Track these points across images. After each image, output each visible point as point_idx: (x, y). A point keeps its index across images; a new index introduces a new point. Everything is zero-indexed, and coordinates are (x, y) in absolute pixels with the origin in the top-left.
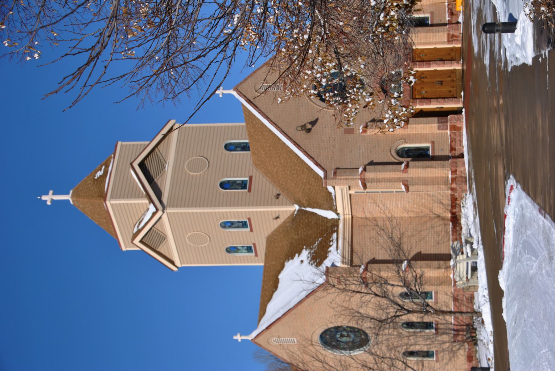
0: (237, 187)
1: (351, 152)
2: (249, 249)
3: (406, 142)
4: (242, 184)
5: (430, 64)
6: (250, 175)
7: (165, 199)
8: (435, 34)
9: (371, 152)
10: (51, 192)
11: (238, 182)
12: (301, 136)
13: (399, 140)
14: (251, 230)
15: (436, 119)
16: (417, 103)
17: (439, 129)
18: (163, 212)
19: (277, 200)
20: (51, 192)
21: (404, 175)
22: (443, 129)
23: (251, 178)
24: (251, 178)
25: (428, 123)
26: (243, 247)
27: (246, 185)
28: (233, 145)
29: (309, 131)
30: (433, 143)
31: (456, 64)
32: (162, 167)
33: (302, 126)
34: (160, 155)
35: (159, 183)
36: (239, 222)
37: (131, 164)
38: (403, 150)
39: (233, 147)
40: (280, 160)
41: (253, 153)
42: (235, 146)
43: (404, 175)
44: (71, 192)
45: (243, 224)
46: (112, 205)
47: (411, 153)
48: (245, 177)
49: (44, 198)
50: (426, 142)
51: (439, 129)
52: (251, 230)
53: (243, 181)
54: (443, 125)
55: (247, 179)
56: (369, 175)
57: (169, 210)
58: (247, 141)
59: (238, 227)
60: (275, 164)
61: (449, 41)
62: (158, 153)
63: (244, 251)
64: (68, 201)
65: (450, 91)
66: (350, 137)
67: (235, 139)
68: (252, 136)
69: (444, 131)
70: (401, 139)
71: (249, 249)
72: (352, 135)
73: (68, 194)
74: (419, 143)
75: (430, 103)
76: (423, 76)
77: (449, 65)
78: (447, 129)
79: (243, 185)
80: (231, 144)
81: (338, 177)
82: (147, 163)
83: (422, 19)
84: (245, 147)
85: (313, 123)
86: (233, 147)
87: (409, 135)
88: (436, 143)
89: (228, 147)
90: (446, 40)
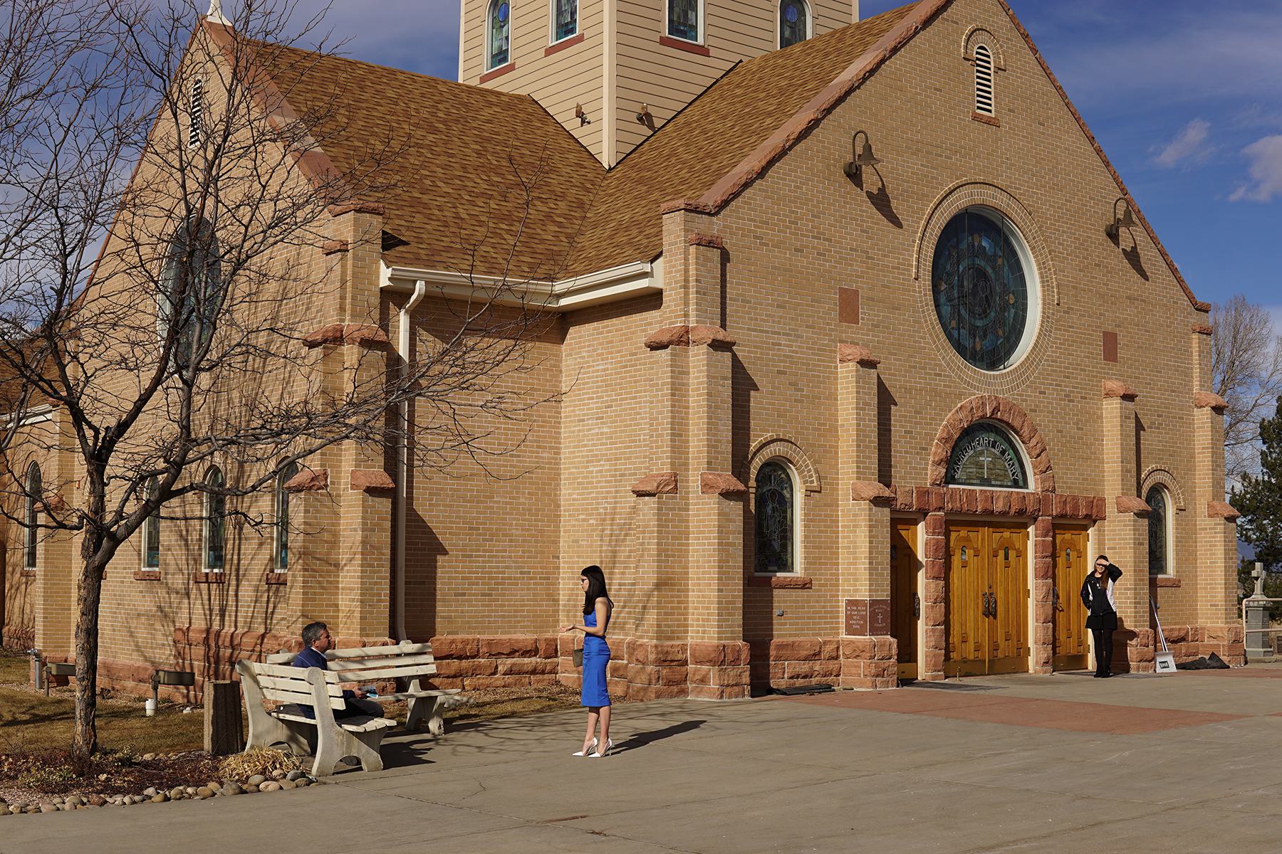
0: (676, 9)
1: (778, 306)
2: (500, 56)
3: (809, 492)
4: (685, 25)
5: (1045, 577)
6: (713, 52)
8: (1130, 593)
9: (779, 372)
11: (691, 15)
13: (817, 471)
14: (550, 51)
15: (885, 595)
16: (934, 533)
19: (634, 117)
21: (694, 480)
23: (703, 51)
24: (703, 51)
25: (872, 568)
26: (507, 38)
27: (684, 34)
28: (799, 18)
29: (854, 175)
30: (805, 585)
31: (1043, 656)
33: (868, 148)
36: (573, 13)
38: (782, 481)
39: (792, 17)
41: (775, 56)
42: (795, 23)
45: (567, 24)
47: (774, 510)
48: (705, 36)
50: (810, 561)
52: (550, 51)
53: (694, 28)
54: (863, 618)
55: (700, 41)
56: (698, 357)
58: (809, 36)
59: (560, 13)
63: (496, 44)
69: (842, 619)
70: (819, 479)
71: (500, 56)
72: (835, 315)
76: (1012, 554)
77: (1041, 635)
79: (682, 25)
81: (693, 249)
83: (1161, 552)
87: (834, 504)
88: (805, 593)
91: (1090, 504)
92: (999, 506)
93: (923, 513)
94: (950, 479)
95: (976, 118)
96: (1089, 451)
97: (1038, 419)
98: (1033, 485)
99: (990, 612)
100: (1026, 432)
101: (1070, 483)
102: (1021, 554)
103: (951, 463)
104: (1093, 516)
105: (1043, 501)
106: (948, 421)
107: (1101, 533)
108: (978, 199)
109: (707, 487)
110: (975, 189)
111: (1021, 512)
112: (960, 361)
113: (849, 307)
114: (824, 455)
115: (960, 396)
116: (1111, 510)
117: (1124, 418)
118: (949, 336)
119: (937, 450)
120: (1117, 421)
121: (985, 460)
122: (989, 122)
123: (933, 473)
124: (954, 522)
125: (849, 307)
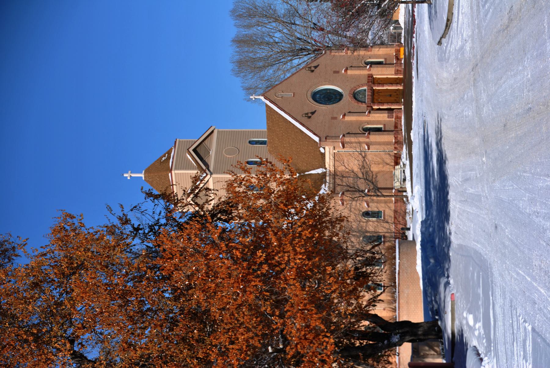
3: (368, 124)
7: (211, 169)
10: (130, 172)
12: (304, 120)
15: (387, 111)
17: (388, 118)
18: (211, 176)
20: (130, 172)
21: (367, 140)
22: (391, 118)
25: (382, 113)
29: (310, 117)
31: (399, 86)
32: (208, 152)
33: (306, 114)
34: (206, 146)
35: (206, 160)
37: (188, 149)
40: (289, 141)
43: (367, 140)
44: (144, 172)
46: (175, 174)
49: (125, 175)
50: (380, 124)
51: (388, 118)
56: (347, 139)
57: (214, 176)
60: (285, 145)
61: (396, 74)
62: (205, 145)
64: (142, 177)
65: (395, 100)
66: (335, 121)
67: (255, 138)
68: (270, 129)
73: (141, 173)
74: (377, 125)
75: (383, 105)
78: (393, 118)
80: (253, 141)
82: (198, 149)
84: (263, 143)
85: (313, 113)
86: (255, 143)
87: (370, 121)
89: (250, 142)
90: (393, 73)
91: (369, 77)
92: (370, 94)
93: (371, 107)
94: (365, 102)
95: (294, 96)
96: (359, 76)
97: (352, 86)
98: (365, 88)
99: (391, 95)
100: (355, 89)
101: (365, 81)
102: (379, 90)
103: (362, 102)
104: (371, 76)
105: (368, 86)
106: (354, 102)
107: (375, 75)
108: (310, 97)
109: (368, 138)
110: (308, 97)
111: (371, 90)
112: (342, 100)
113: (335, 118)
114: (362, 122)
115: (349, 100)
116: (370, 73)
117: (351, 70)
118: (337, 102)
119: (360, 104)
120: (352, 71)
121: (361, 96)
122: (294, 94)
123: (364, 105)
124: (373, 101)
125: (335, 118)
